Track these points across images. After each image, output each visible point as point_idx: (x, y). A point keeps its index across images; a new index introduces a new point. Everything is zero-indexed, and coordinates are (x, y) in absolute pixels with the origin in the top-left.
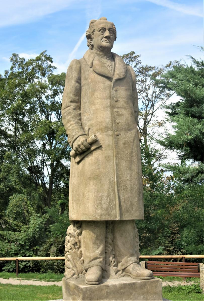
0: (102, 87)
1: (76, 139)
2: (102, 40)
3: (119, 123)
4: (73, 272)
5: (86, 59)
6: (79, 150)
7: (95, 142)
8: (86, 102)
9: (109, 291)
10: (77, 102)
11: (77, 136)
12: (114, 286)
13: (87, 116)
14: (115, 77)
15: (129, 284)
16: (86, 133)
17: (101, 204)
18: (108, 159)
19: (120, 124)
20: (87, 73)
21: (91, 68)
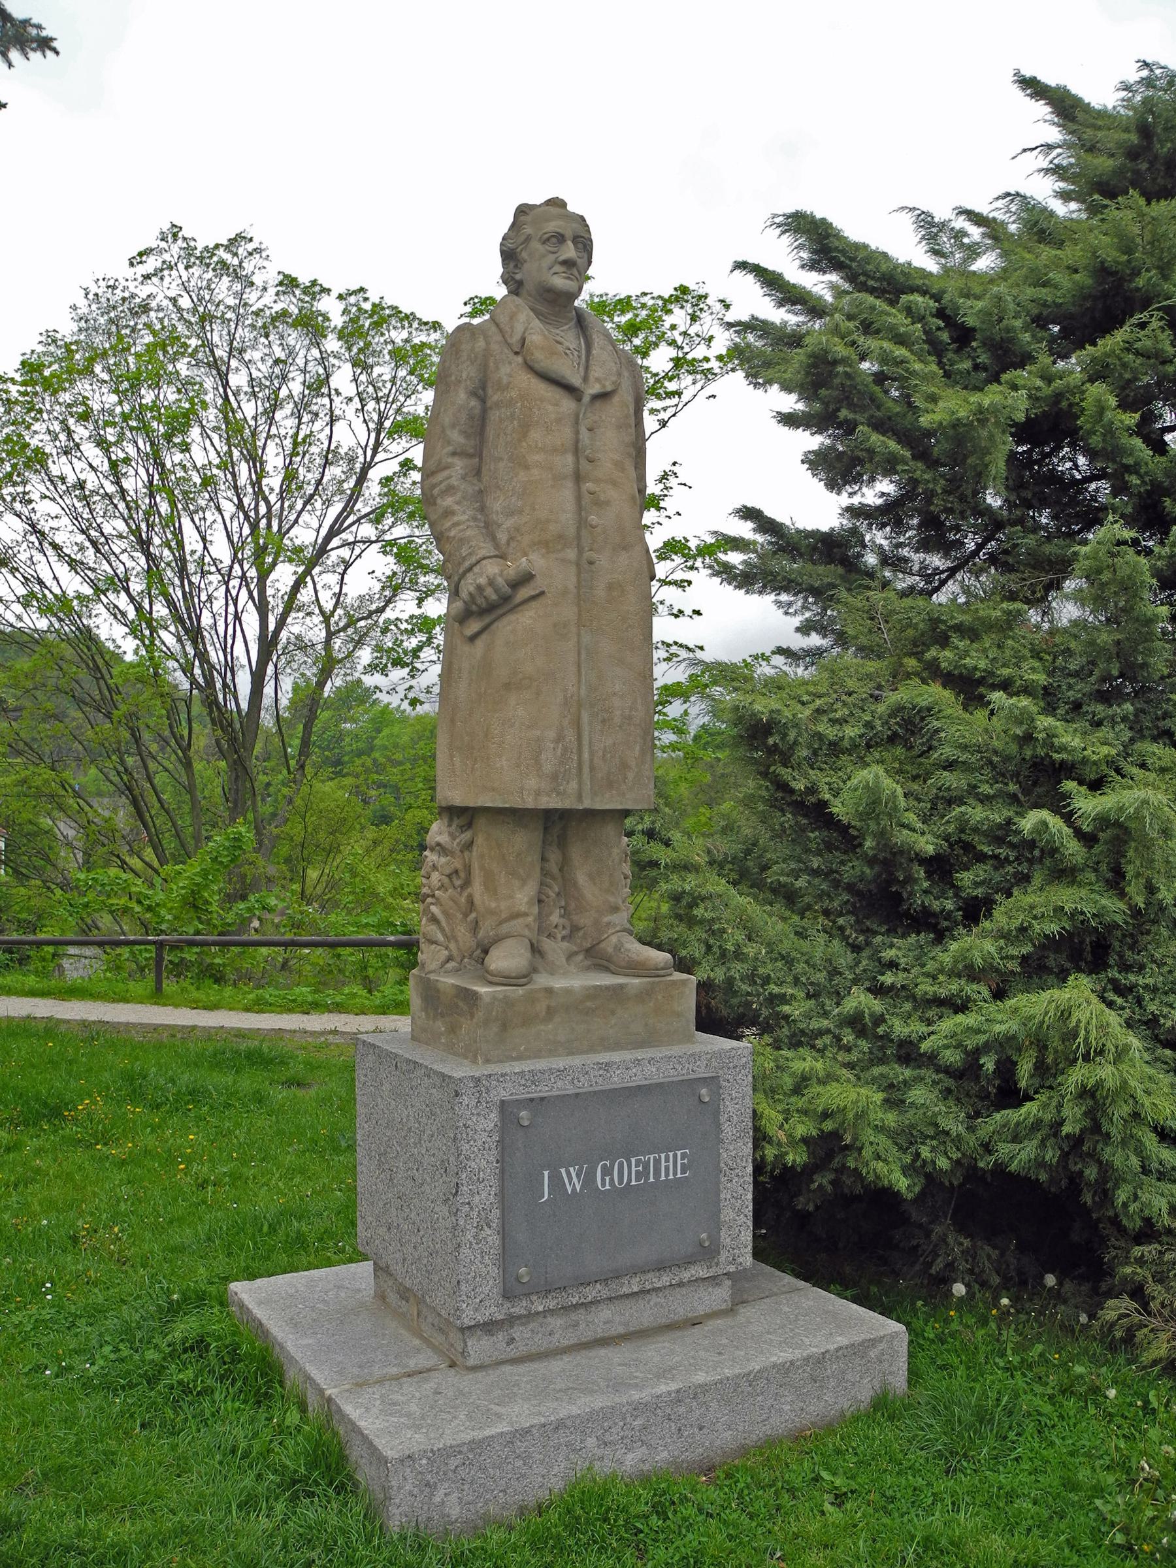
0: (553, 416)
1: (470, 569)
2: (553, 270)
5: (502, 326)
6: (480, 601)
7: (526, 578)
8: (501, 459)
9: (553, 1004)
10: (471, 456)
12: (568, 991)
13: (502, 498)
17: (537, 761)
19: (599, 530)
20: (504, 370)
21: (517, 353)
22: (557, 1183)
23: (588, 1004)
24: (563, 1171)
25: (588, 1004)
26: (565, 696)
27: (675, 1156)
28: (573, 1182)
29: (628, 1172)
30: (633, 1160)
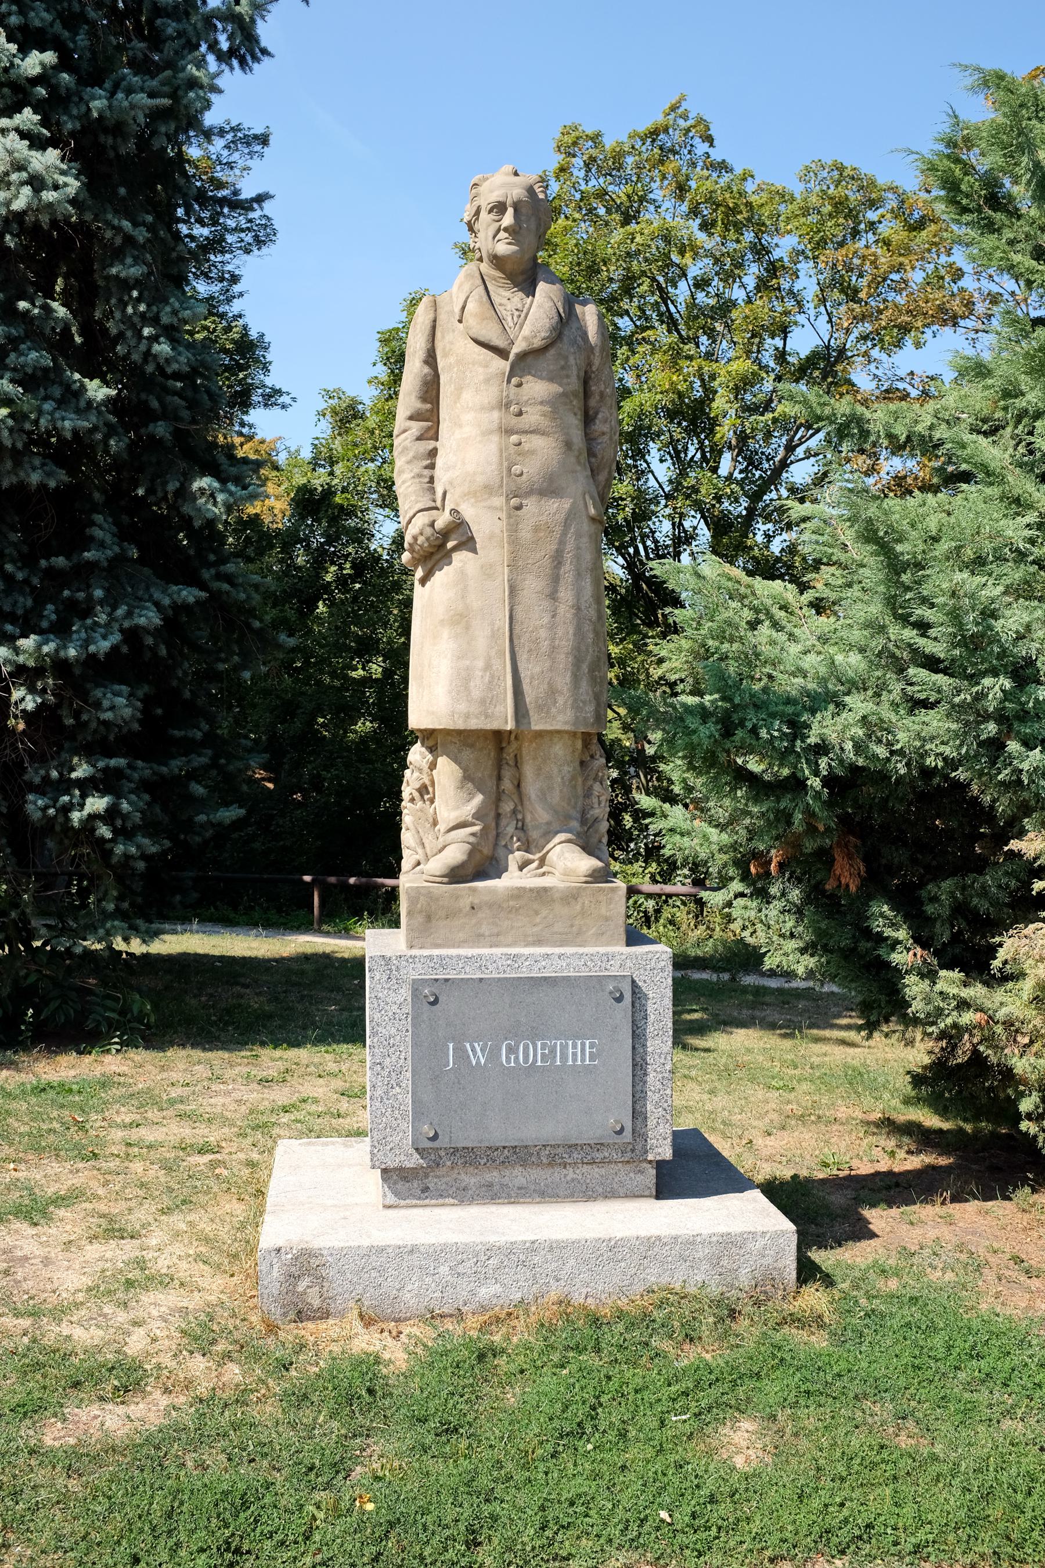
0: (481, 377)
3: (521, 474)
4: (417, 857)
9: (476, 901)
11: (411, 513)
14: (515, 350)
15: (531, 890)
16: (439, 504)
17: (467, 689)
18: (487, 572)
20: (449, 337)
22: (461, 1054)
23: (511, 903)
24: (468, 1045)
25: (511, 903)
26: (492, 630)
27: (583, 1045)
28: (478, 1056)
29: (534, 1053)
30: (539, 1044)
